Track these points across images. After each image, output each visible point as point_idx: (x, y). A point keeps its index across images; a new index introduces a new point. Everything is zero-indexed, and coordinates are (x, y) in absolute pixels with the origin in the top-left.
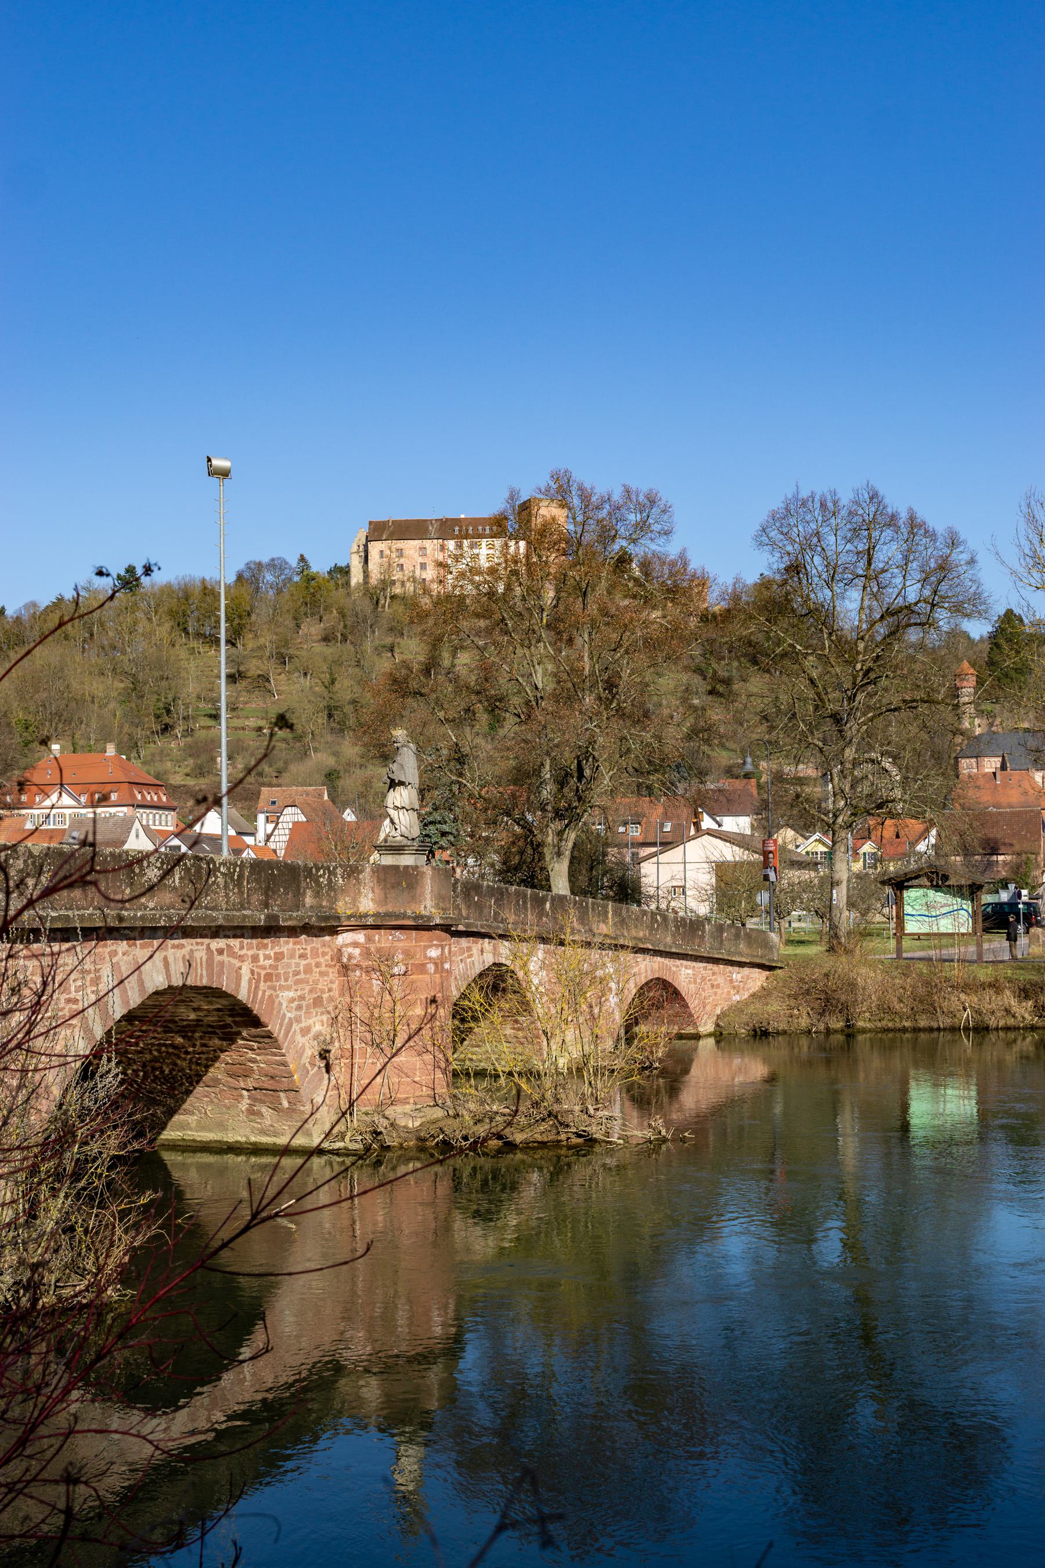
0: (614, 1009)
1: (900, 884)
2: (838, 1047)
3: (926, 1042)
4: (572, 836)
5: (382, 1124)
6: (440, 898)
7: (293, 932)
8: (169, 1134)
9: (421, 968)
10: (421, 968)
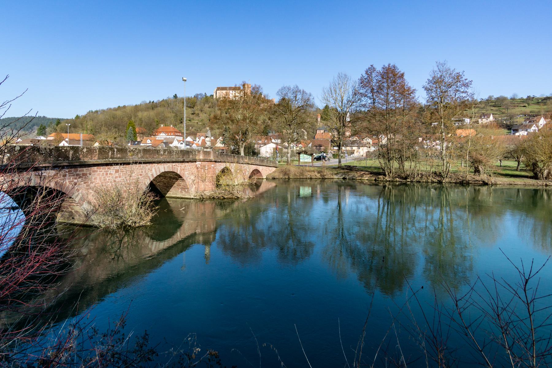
0: (248, 174)
1: (299, 153)
2: (287, 181)
3: (302, 180)
4: (244, 144)
5: (203, 194)
6: (214, 156)
7: (188, 162)
8: (167, 195)
9: (210, 168)
10: (210, 168)
